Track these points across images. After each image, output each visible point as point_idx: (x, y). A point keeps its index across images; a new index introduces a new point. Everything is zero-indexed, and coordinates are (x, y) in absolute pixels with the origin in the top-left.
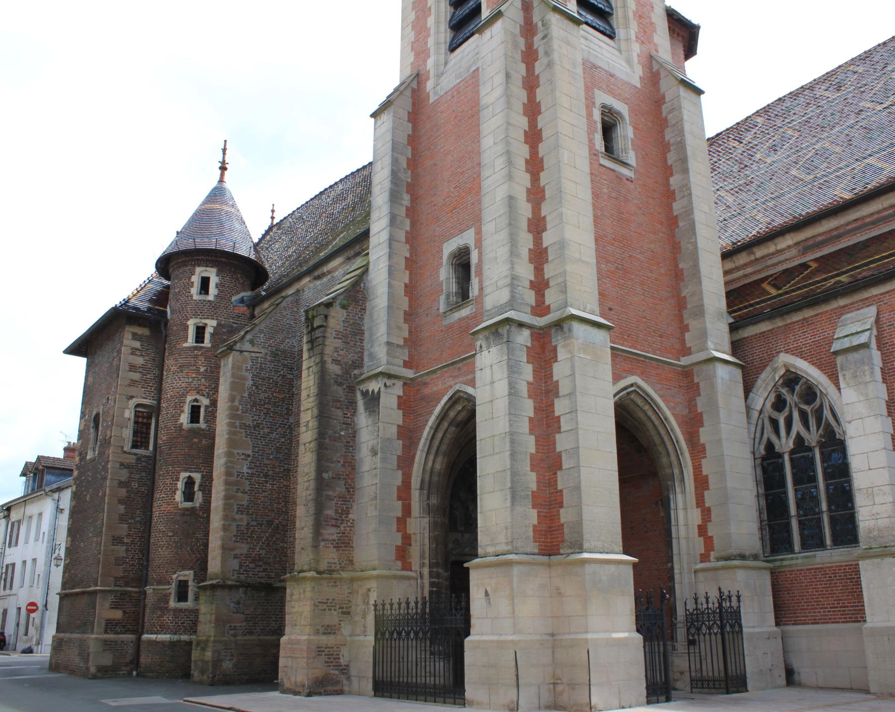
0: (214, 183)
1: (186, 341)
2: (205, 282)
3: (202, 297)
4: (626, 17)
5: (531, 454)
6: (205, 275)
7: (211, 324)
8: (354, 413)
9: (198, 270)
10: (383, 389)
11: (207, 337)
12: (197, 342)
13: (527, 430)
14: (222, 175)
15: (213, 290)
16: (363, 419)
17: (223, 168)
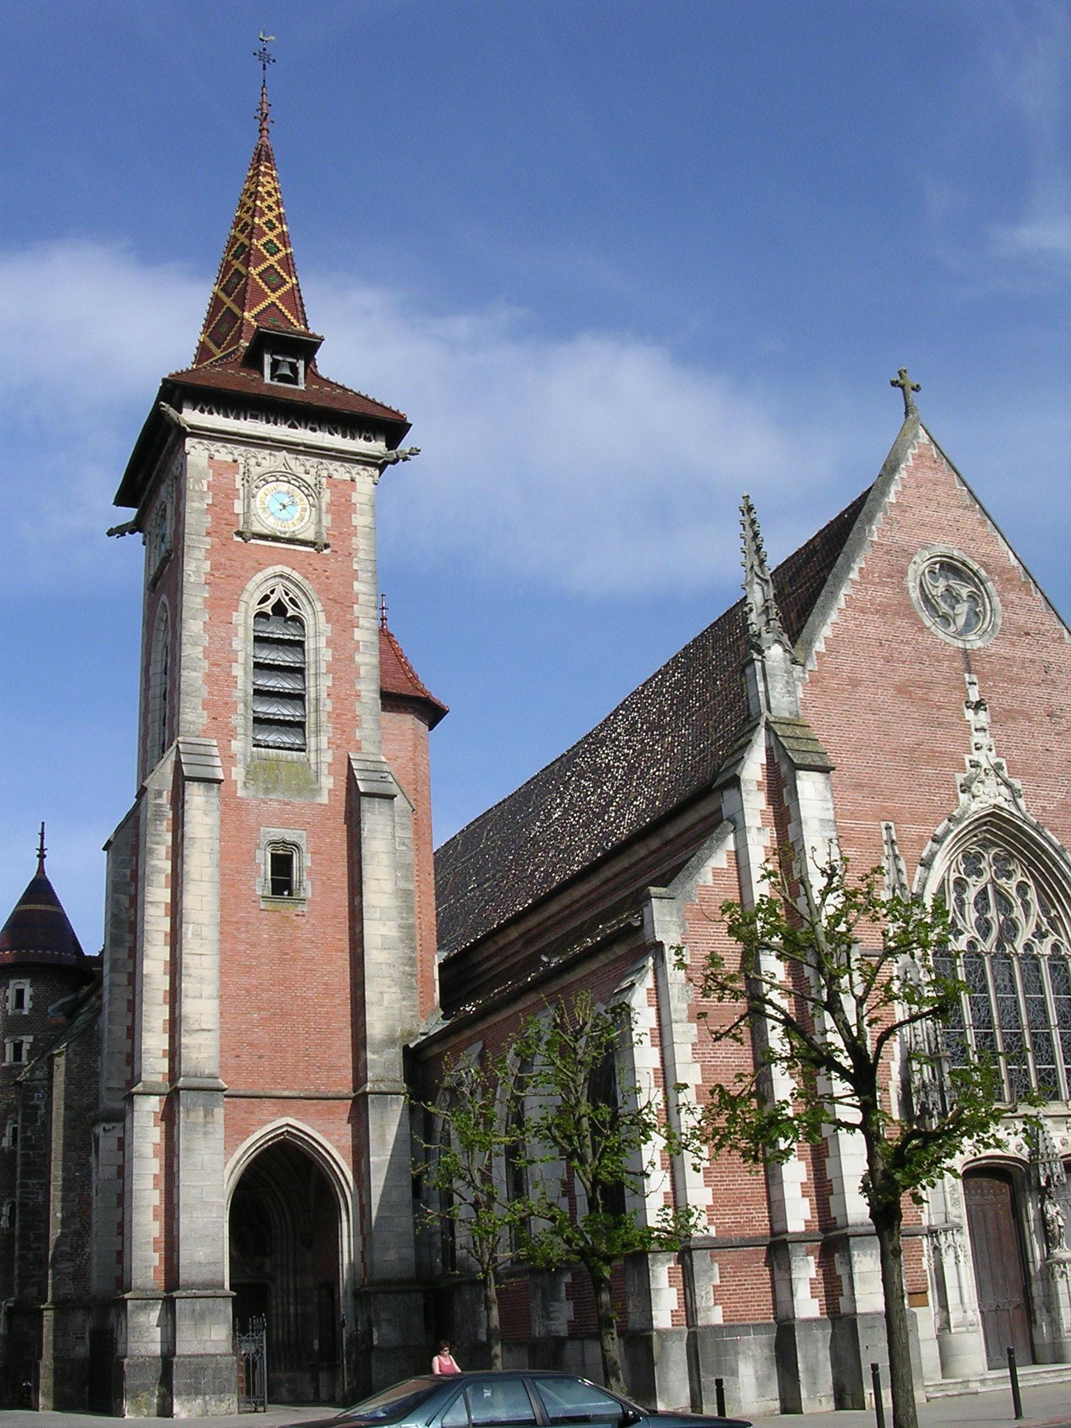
0: (32, 875)
1: (4, 1061)
2: (20, 994)
3: (18, 1011)
4: (317, 724)
5: (155, 1206)
6: (20, 987)
7: (28, 1039)
8: (89, 1154)
9: (12, 982)
10: (102, 1133)
11: (24, 1053)
12: (15, 1060)
13: (152, 1186)
14: (41, 863)
15: (27, 1003)
16: (92, 1159)
17: (42, 856)
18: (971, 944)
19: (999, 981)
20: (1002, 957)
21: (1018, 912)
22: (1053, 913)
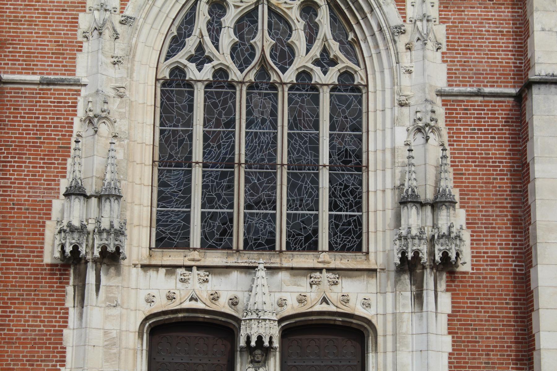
18: (221, 72)
19: (256, 114)
20: (263, 87)
21: (298, 38)
22: (351, 36)
